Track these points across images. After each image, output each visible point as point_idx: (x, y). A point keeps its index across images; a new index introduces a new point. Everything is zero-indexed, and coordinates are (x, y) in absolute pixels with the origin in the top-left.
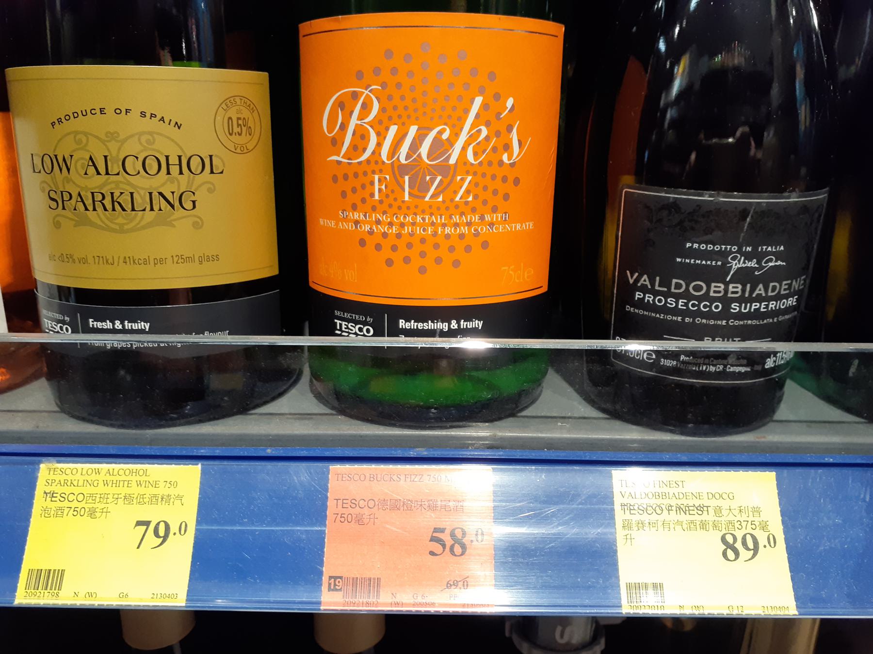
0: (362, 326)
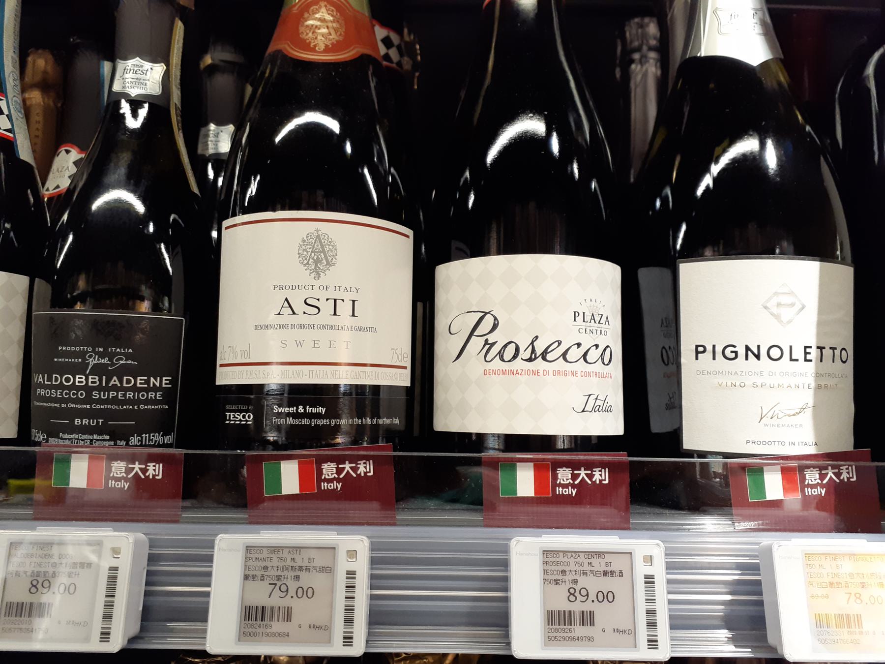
0: (245, 414)
